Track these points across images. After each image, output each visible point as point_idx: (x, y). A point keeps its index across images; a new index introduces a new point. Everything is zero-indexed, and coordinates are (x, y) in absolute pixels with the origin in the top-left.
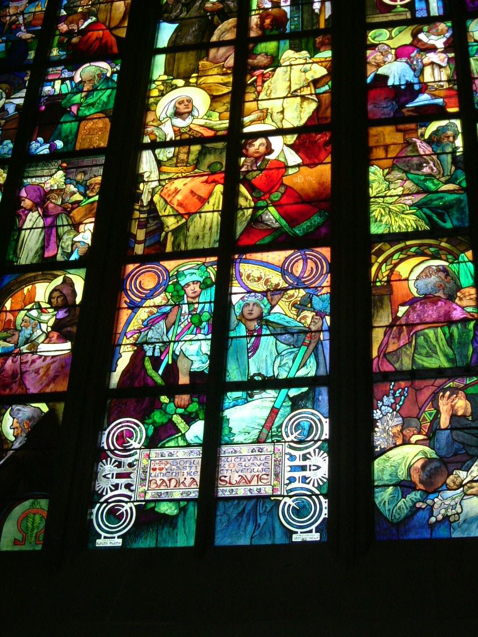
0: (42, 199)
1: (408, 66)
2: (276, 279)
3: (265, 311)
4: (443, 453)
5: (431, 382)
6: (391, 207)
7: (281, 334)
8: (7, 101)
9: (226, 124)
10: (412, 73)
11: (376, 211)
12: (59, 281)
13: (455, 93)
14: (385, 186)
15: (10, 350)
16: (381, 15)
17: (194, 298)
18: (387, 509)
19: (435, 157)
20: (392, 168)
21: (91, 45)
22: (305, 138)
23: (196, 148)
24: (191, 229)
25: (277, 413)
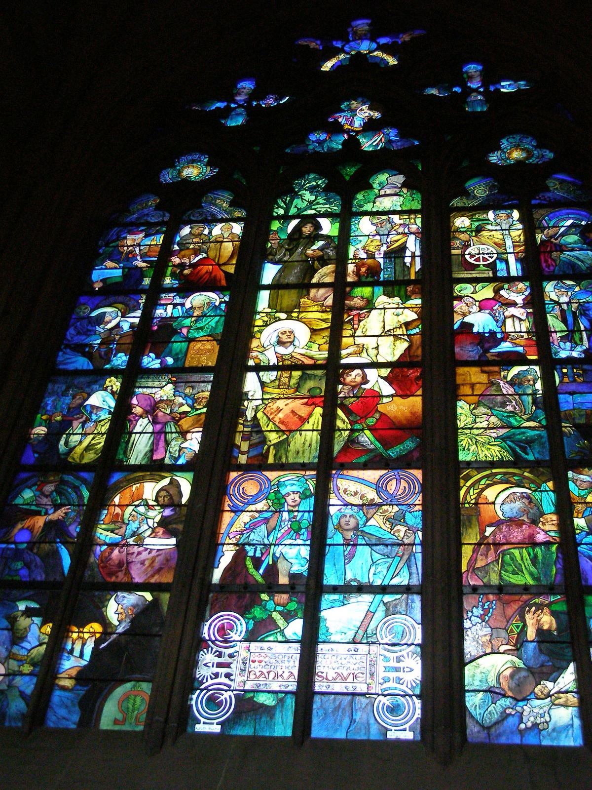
0: (152, 409)
2: (371, 495)
3: (361, 523)
4: (531, 663)
5: (517, 597)
6: (477, 437)
7: (376, 545)
9: (325, 354)
11: (463, 440)
12: (165, 482)
13: (534, 343)
14: (471, 419)
15: (117, 541)
18: (478, 713)
19: (517, 397)
20: (478, 404)
21: (201, 278)
22: (398, 372)
23: (297, 374)
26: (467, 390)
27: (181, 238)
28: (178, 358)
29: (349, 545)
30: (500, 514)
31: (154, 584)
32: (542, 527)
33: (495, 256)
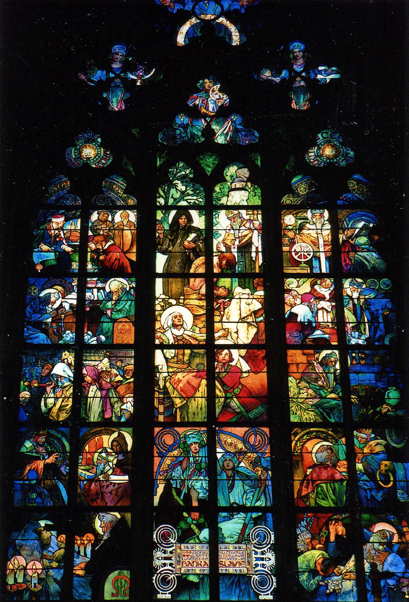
0: (98, 377)
1: (308, 308)
2: (240, 445)
3: (236, 465)
4: (332, 555)
5: (324, 515)
6: (301, 405)
8: (63, 300)
9: (204, 337)
10: (311, 314)
11: (293, 407)
12: (115, 435)
13: (335, 331)
14: (296, 391)
15: (93, 478)
16: (292, 268)
17: (196, 453)
19: (324, 375)
20: (301, 379)
21: (113, 264)
23: (188, 352)
24: (190, 407)
25: (247, 527)
26: (293, 368)
27: (93, 223)
28: (108, 336)
29: (230, 480)
30: (315, 460)
31: (121, 507)
32: (338, 469)
33: (312, 254)
